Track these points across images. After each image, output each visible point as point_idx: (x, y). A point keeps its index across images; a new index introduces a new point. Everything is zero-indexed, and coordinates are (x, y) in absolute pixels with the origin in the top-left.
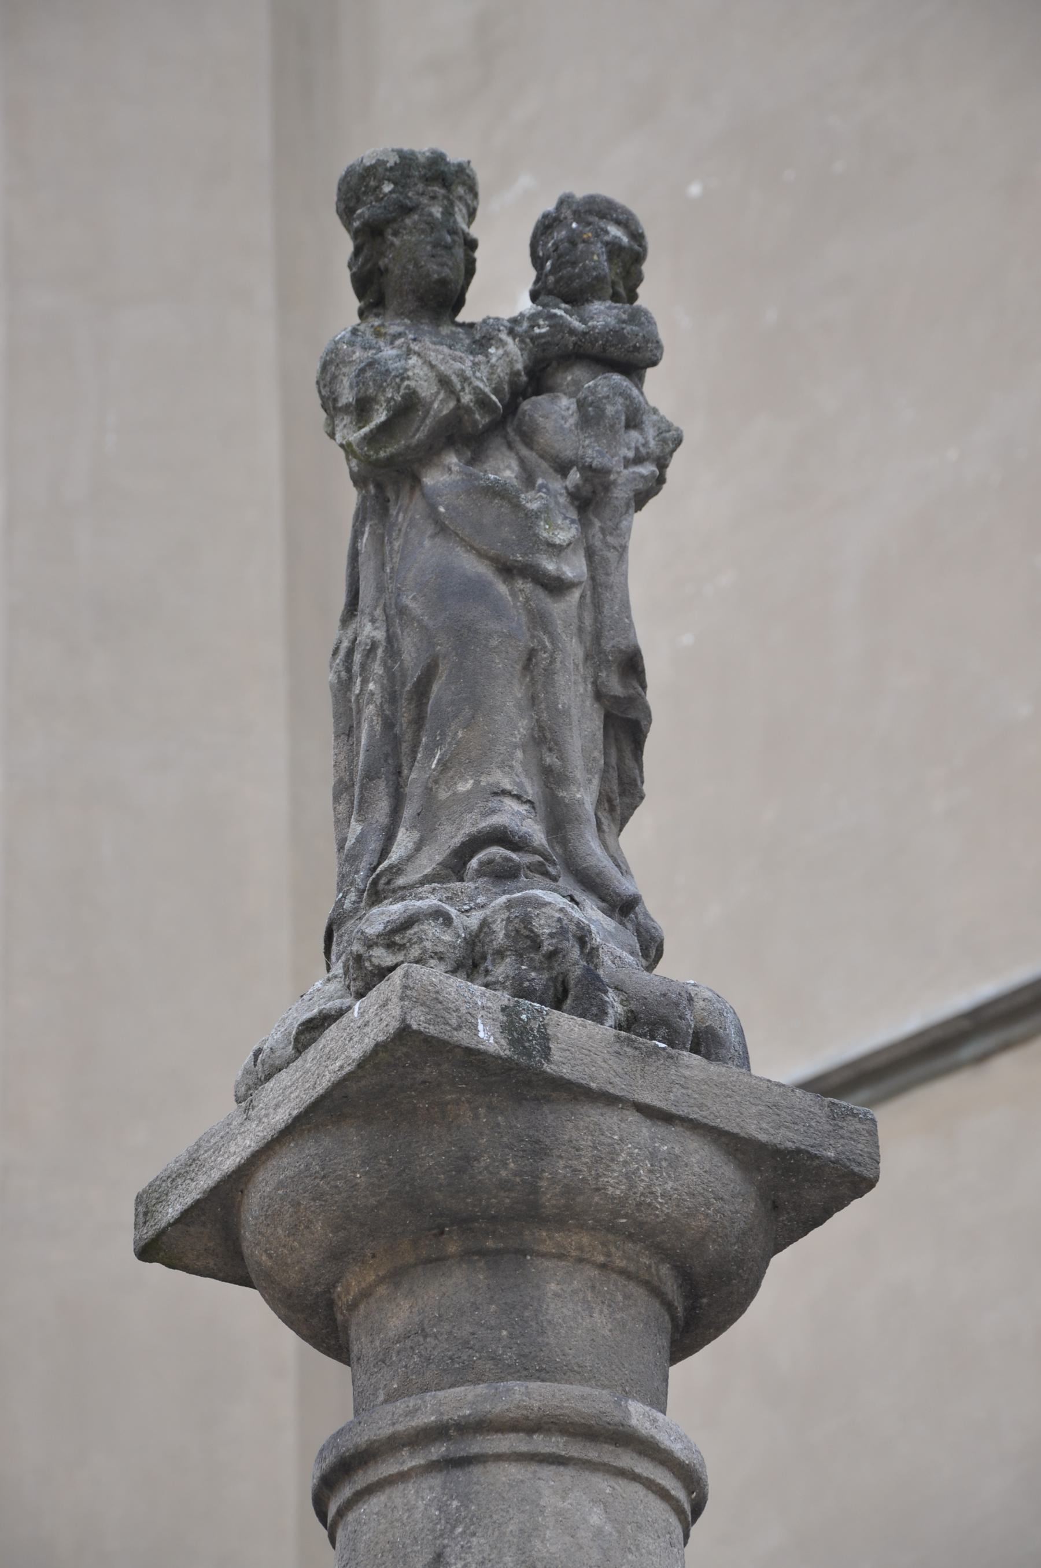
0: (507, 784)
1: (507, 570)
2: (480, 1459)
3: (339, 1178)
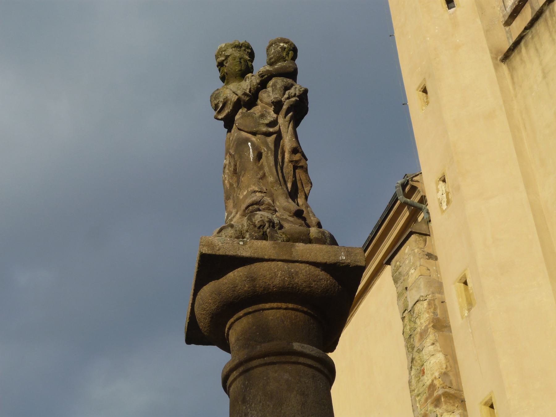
0: (256, 189)
1: (254, 134)
2: (253, 368)
3: (206, 303)
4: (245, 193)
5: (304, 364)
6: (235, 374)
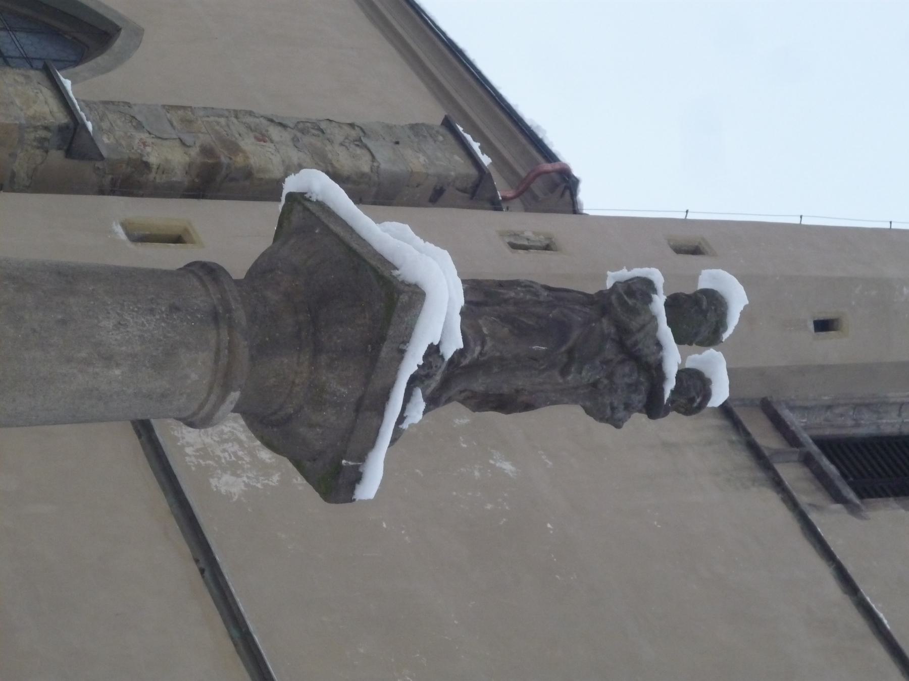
0: (486, 348)
1: (570, 352)
4: (485, 330)
5: (207, 400)
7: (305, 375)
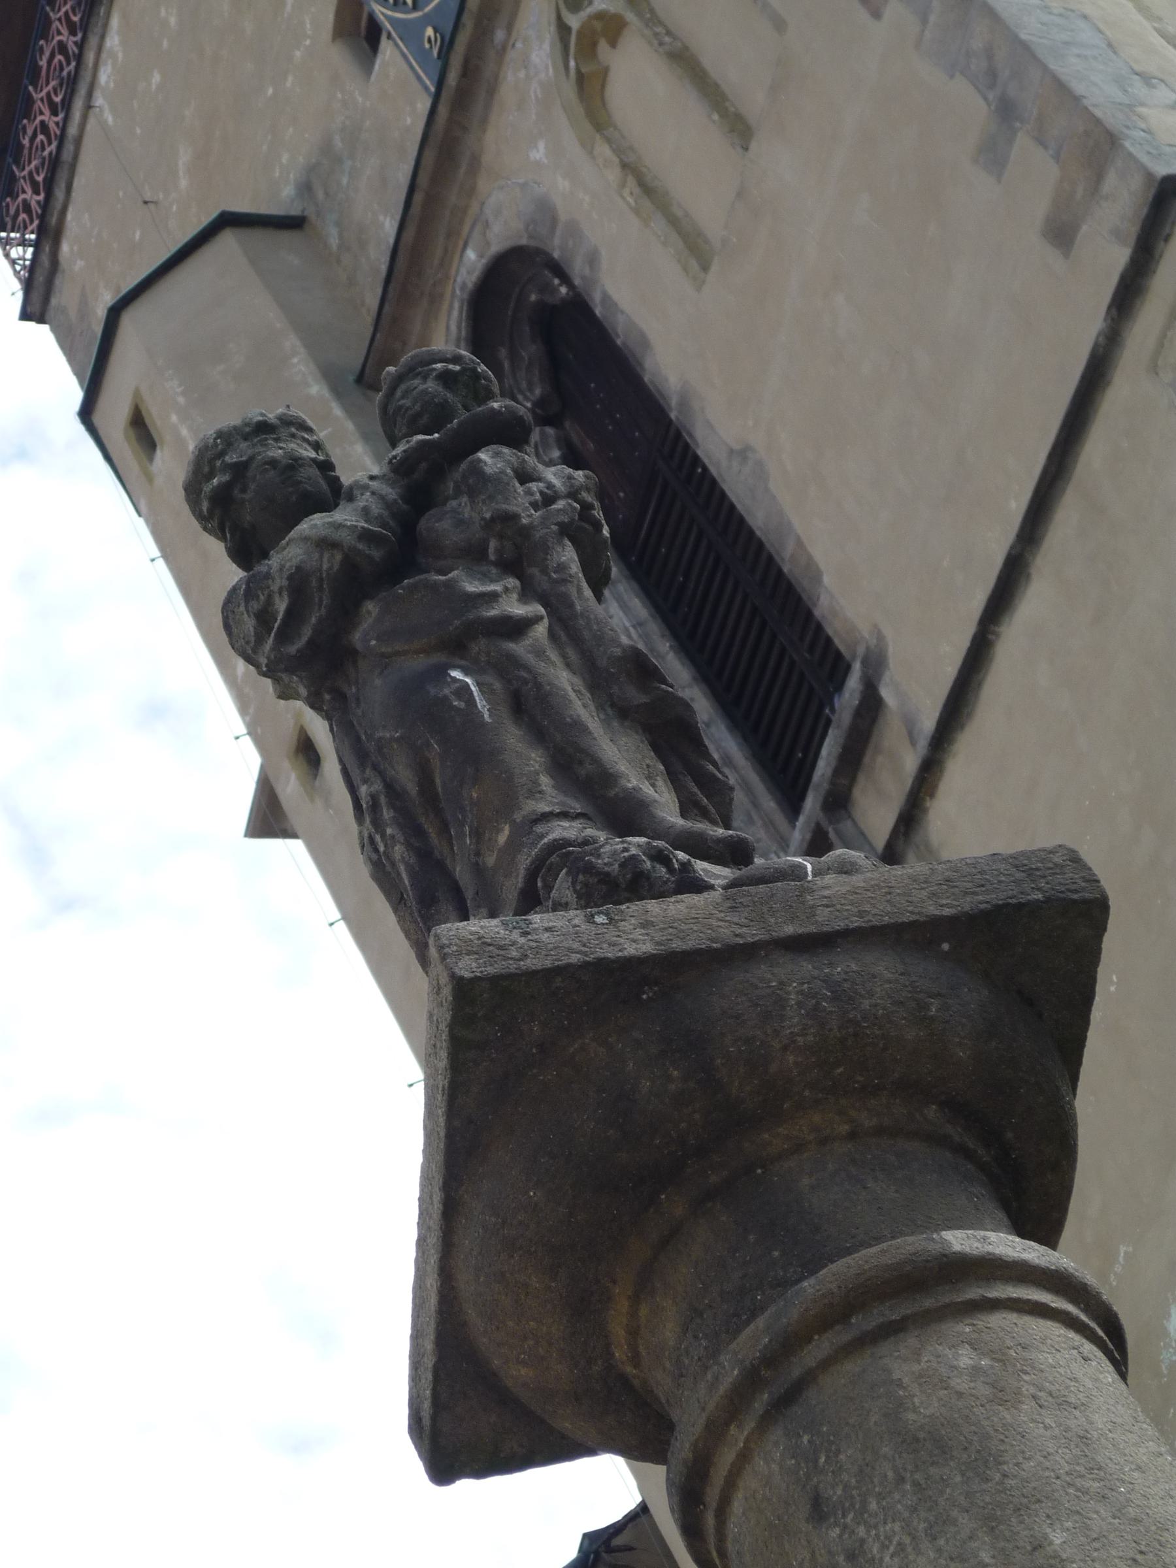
0: (544, 807)
4: (502, 838)
6: (738, 1435)
7: (817, 1118)
